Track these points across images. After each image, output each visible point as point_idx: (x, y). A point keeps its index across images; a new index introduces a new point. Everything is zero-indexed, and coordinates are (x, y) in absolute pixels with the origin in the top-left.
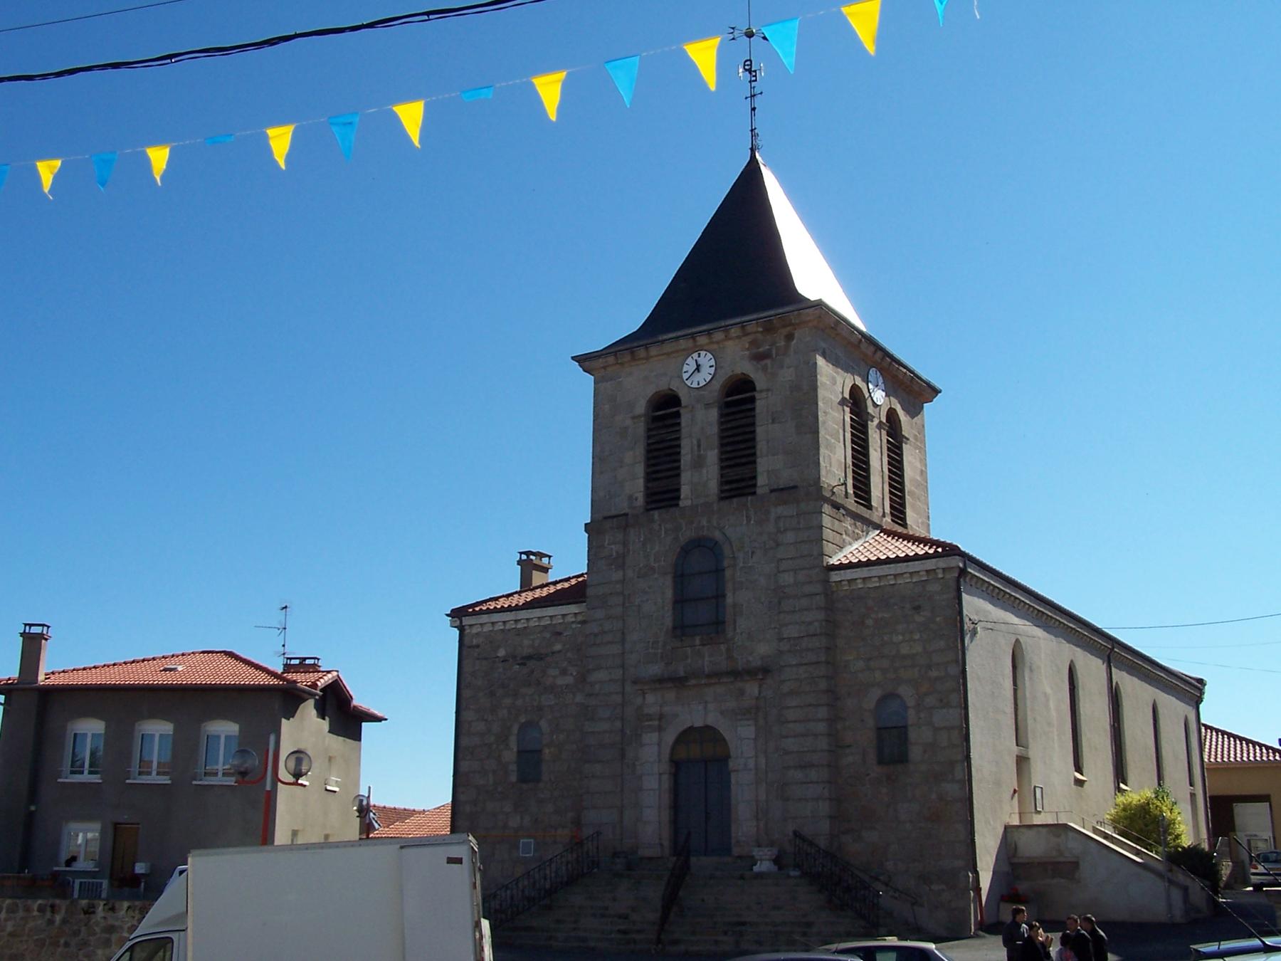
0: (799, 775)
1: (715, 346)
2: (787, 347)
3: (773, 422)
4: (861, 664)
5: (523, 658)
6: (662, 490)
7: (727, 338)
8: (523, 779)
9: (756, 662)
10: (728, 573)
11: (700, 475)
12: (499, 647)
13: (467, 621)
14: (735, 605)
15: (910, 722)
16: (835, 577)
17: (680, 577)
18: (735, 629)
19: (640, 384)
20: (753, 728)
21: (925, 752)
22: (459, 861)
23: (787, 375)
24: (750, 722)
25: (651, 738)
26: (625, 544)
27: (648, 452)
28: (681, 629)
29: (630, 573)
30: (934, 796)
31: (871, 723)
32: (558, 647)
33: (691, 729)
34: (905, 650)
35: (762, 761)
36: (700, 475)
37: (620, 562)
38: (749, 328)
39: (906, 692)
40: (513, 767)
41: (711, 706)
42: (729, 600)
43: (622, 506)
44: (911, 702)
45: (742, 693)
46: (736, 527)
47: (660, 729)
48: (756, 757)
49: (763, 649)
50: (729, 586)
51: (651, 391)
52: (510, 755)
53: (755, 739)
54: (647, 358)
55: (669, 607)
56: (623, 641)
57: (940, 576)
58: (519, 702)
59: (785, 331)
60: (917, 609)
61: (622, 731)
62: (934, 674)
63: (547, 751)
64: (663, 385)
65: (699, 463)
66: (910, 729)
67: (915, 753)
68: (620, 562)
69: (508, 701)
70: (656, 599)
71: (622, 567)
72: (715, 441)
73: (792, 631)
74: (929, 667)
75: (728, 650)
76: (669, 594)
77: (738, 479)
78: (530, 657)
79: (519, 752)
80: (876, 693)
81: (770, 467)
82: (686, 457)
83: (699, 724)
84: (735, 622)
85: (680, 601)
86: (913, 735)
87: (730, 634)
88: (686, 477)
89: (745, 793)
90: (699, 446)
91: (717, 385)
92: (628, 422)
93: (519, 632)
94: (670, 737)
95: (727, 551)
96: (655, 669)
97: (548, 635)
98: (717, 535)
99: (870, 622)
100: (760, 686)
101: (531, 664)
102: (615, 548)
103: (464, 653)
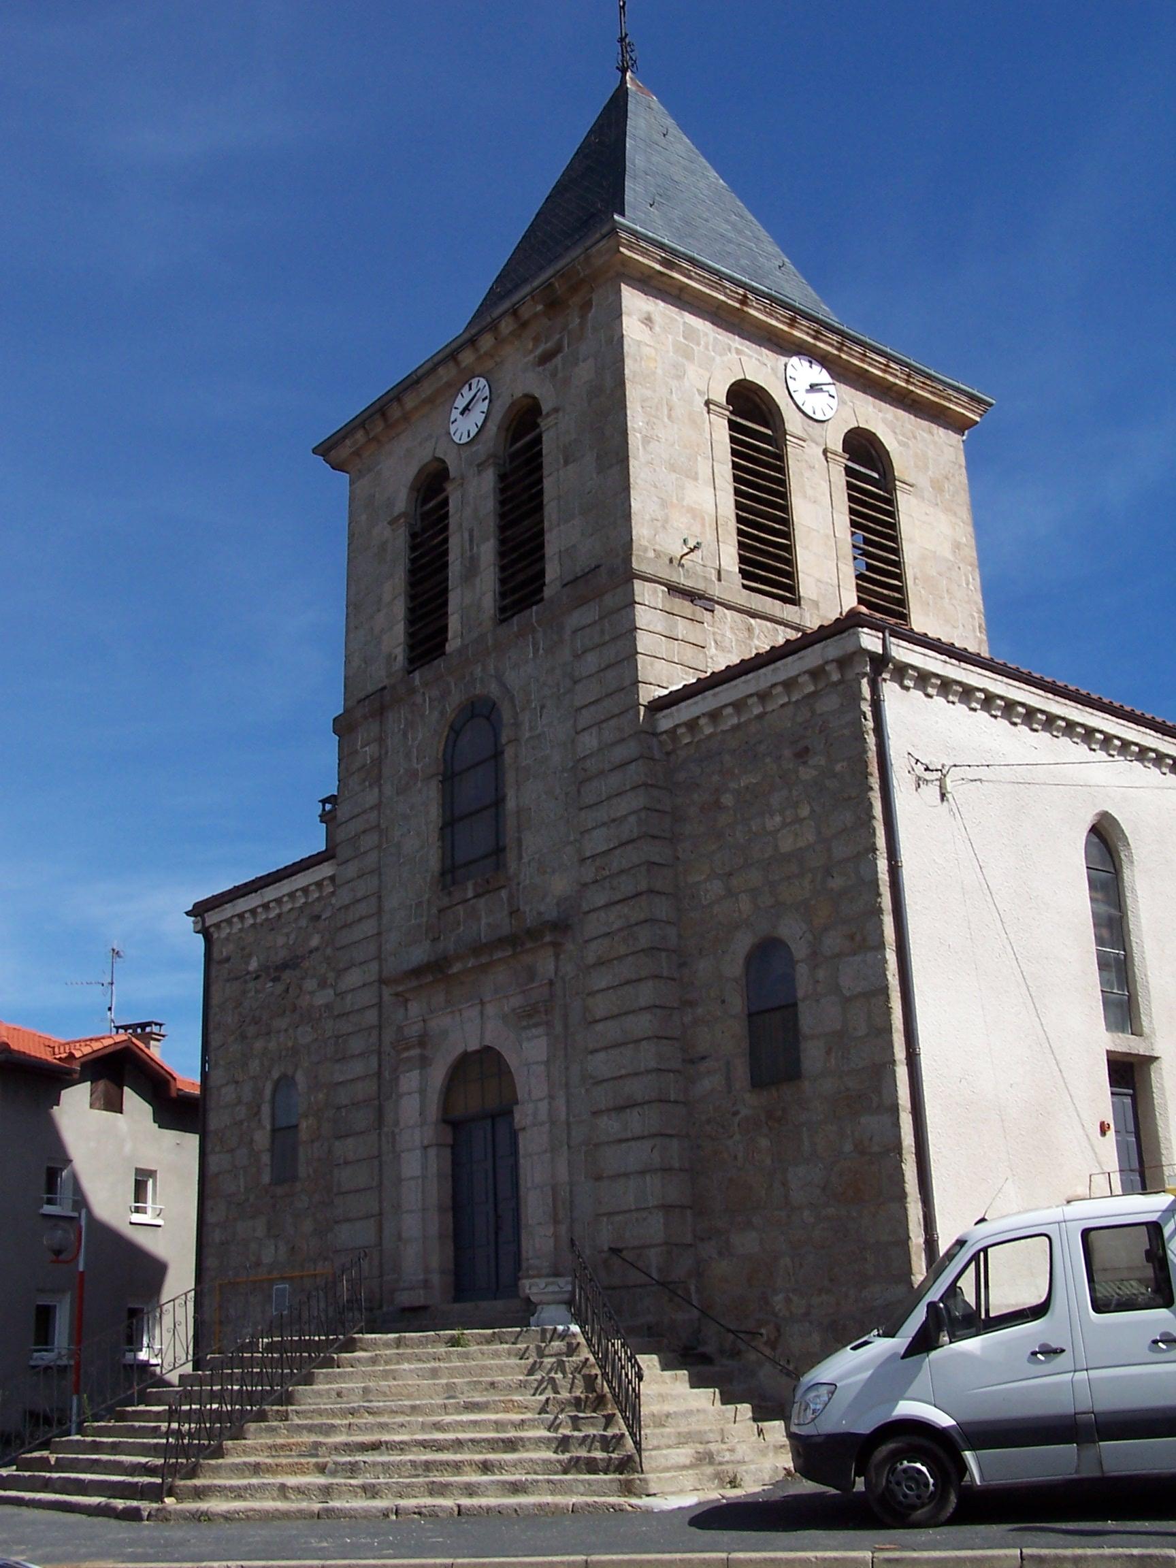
0: (610, 1125)
1: (490, 364)
2: (582, 325)
3: (566, 463)
4: (716, 887)
5: (277, 968)
6: (426, 637)
7: (500, 341)
8: (277, 1180)
9: (550, 911)
10: (509, 753)
11: (473, 594)
12: (250, 956)
13: (212, 918)
14: (518, 812)
15: (800, 994)
16: (665, 722)
17: (449, 777)
18: (520, 858)
19: (397, 472)
20: (543, 1041)
21: (828, 1052)
22: (44, 1335)
23: (584, 372)
24: (541, 1030)
25: (410, 1081)
26: (381, 740)
27: (412, 572)
28: (450, 874)
29: (388, 790)
30: (848, 1147)
31: (737, 1004)
32: (315, 941)
33: (465, 1058)
34: (787, 844)
35: (561, 1102)
36: (473, 594)
37: (374, 773)
38: (525, 312)
39: (791, 930)
40: (266, 1158)
41: (490, 1010)
42: (511, 804)
43: (378, 675)
44: (800, 950)
45: (531, 974)
46: (523, 672)
47: (424, 1062)
48: (551, 1097)
49: (560, 885)
50: (510, 777)
51: (411, 471)
52: (262, 1138)
53: (547, 1063)
54: (406, 418)
55: (434, 836)
56: (380, 912)
57: (835, 677)
58: (272, 1045)
59: (576, 300)
60: (803, 754)
61: (379, 1074)
62: (836, 883)
63: (304, 1125)
64: (424, 455)
65: (471, 571)
66: (802, 1007)
67: (813, 1055)
68: (374, 773)
69: (259, 1045)
70: (418, 820)
71: (378, 781)
72: (491, 524)
73: (597, 842)
74: (828, 873)
75: (511, 897)
76: (434, 812)
77: (521, 582)
78: (285, 966)
79: (274, 1131)
80: (743, 943)
81: (564, 542)
82: (455, 568)
83: (473, 1046)
84: (519, 840)
85: (450, 824)
86: (807, 1021)
87: (513, 867)
88: (455, 600)
89: (540, 1167)
90: (471, 540)
91: (492, 428)
92: (387, 533)
93: (273, 925)
94: (438, 1075)
95: (507, 716)
96: (419, 954)
97: (303, 923)
98: (494, 689)
99: (728, 800)
100: (557, 956)
101: (287, 975)
102: (371, 750)
103: (214, 973)
